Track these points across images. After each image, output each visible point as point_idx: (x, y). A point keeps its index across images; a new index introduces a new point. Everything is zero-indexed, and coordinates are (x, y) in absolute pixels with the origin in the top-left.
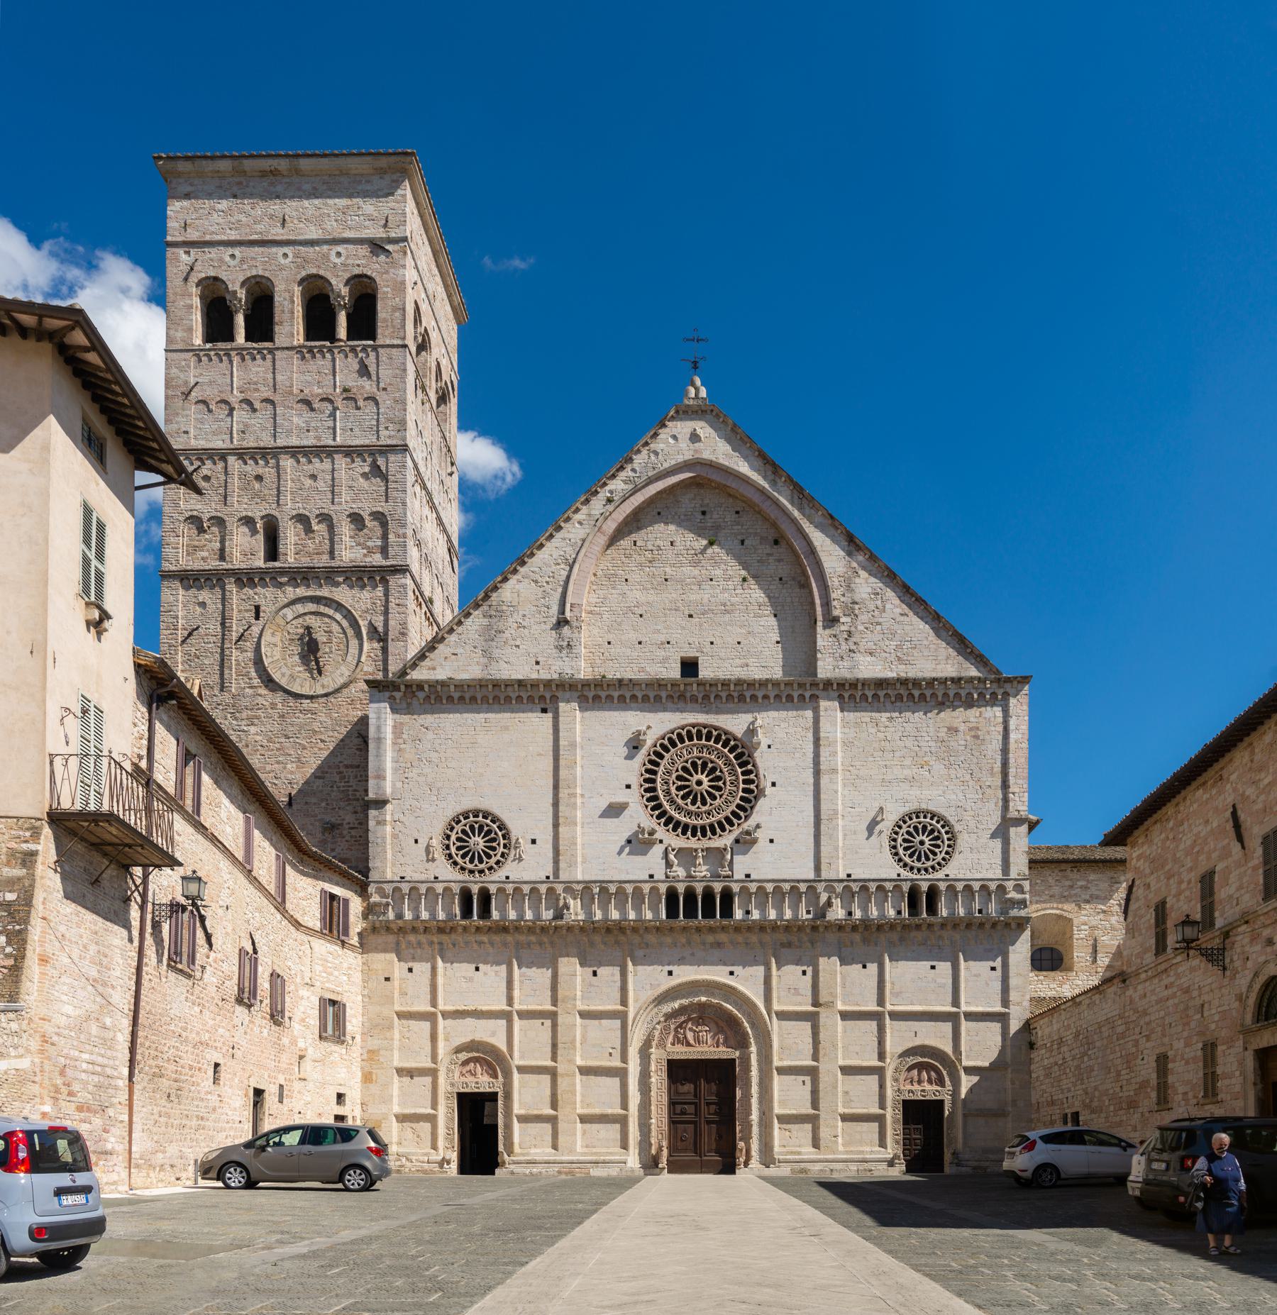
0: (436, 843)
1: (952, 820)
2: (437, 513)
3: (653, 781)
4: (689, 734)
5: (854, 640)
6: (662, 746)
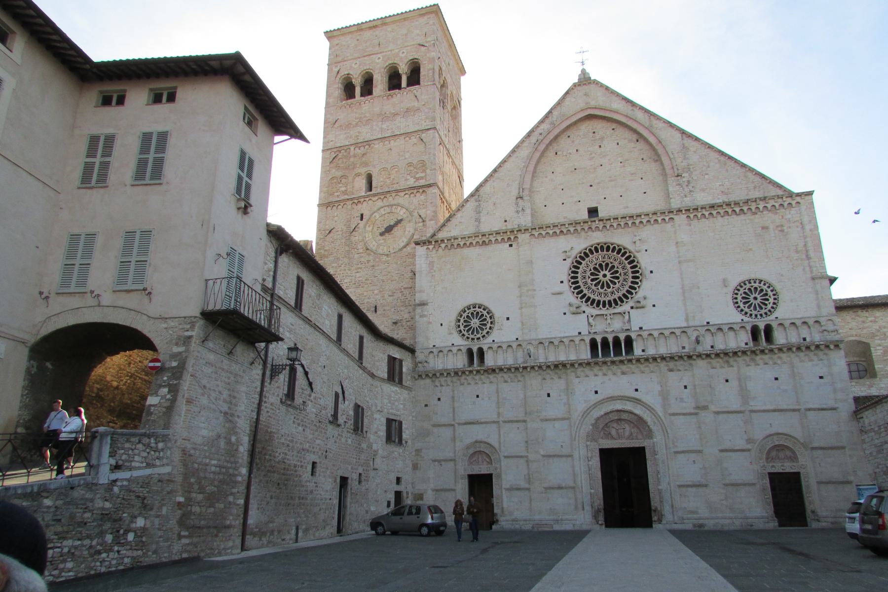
0: (453, 324)
2: (452, 159)
3: (577, 277)
5: (692, 185)
6: (580, 257)
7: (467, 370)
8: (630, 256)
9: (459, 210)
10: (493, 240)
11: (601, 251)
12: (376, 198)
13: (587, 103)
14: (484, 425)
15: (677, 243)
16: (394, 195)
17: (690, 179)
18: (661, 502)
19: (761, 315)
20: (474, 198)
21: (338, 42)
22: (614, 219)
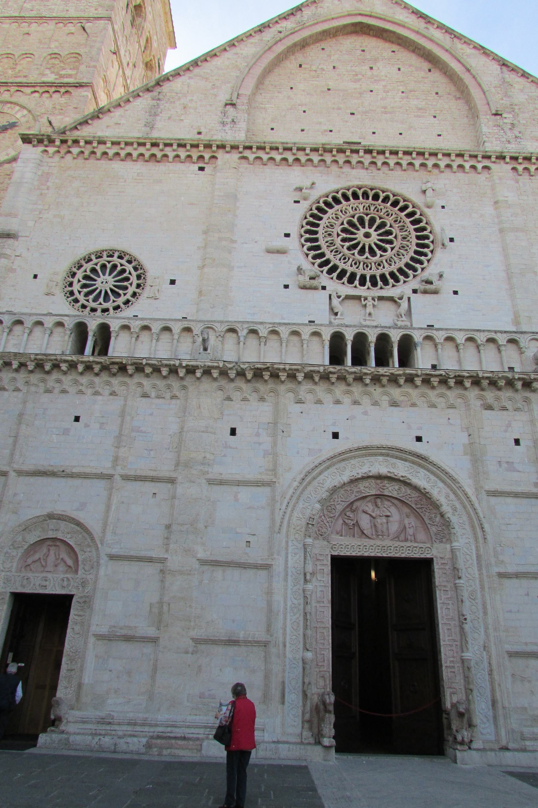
7: (65, 361)
9: (120, 105)
10: (171, 155)
11: (363, 198)
14: (77, 482)
15: (496, 203)
17: (515, 122)
20: (150, 94)
22: (391, 153)
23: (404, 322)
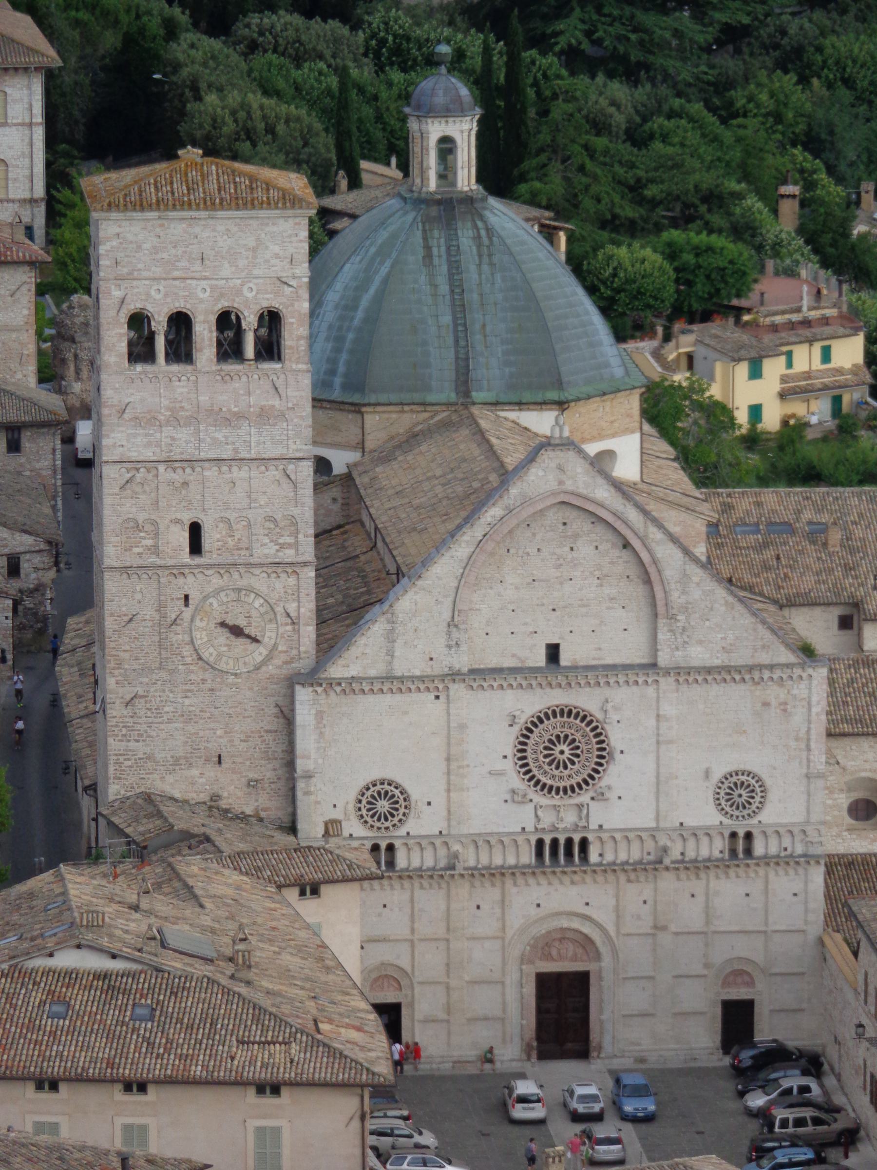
1: (764, 777)
4: (554, 712)
8: (596, 728)
12: (210, 572)
13: (561, 483)
15: (658, 716)
16: (242, 570)
18: (602, 1033)
19: (743, 817)
21: (118, 230)
23: (583, 823)
